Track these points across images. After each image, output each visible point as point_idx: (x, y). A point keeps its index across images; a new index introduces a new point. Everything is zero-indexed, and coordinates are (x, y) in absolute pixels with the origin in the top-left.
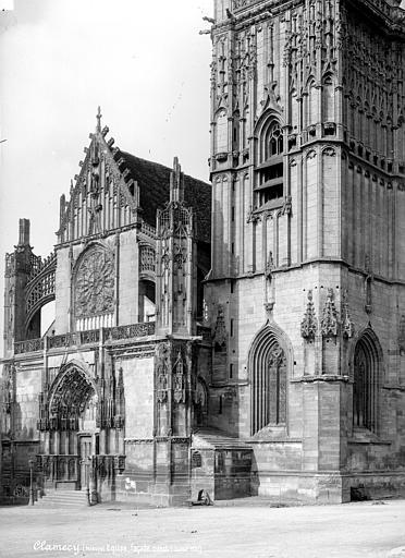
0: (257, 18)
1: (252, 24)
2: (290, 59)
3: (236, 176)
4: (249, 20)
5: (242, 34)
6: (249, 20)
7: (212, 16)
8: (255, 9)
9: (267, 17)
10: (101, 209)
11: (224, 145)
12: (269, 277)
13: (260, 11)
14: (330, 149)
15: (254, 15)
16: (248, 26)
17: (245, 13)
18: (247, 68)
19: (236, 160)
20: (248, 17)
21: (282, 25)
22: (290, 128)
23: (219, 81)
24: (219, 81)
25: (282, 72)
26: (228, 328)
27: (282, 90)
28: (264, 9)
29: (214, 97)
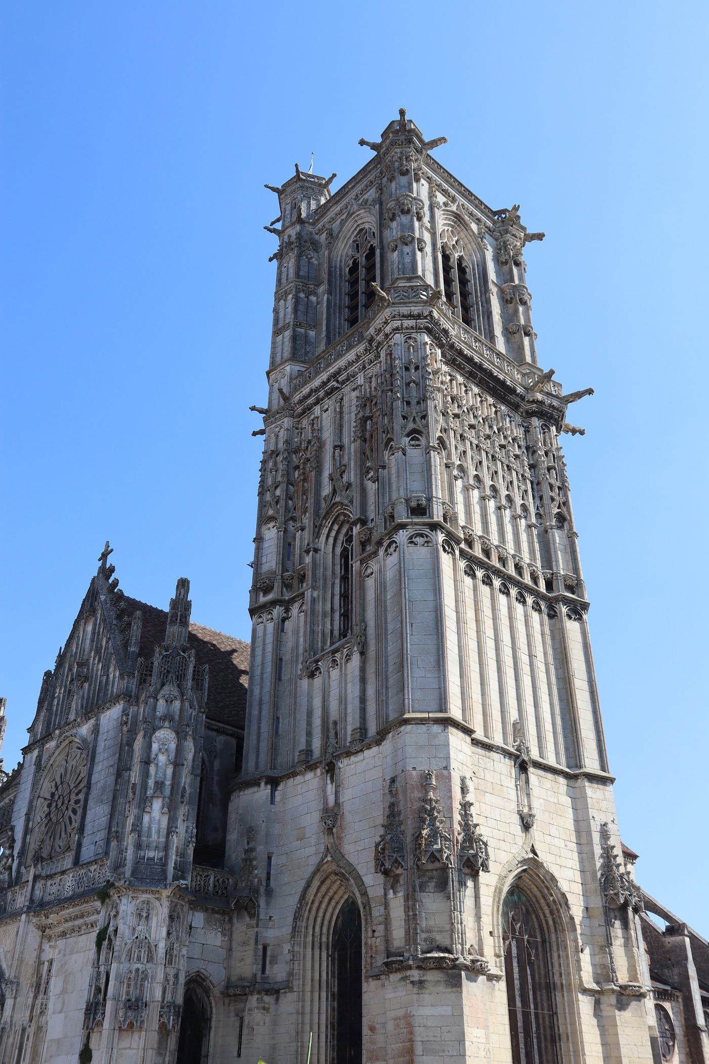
0: (321, 393)
2: (364, 430)
3: (287, 610)
5: (305, 422)
7: (266, 407)
8: (316, 383)
9: (333, 389)
11: (271, 562)
12: (331, 770)
13: (324, 384)
14: (421, 535)
15: (317, 390)
16: (310, 408)
18: (308, 460)
19: (287, 586)
20: (309, 395)
21: (354, 394)
22: (363, 522)
23: (270, 481)
24: (270, 481)
26: (260, 872)
27: (352, 476)
28: (329, 380)
29: (262, 505)
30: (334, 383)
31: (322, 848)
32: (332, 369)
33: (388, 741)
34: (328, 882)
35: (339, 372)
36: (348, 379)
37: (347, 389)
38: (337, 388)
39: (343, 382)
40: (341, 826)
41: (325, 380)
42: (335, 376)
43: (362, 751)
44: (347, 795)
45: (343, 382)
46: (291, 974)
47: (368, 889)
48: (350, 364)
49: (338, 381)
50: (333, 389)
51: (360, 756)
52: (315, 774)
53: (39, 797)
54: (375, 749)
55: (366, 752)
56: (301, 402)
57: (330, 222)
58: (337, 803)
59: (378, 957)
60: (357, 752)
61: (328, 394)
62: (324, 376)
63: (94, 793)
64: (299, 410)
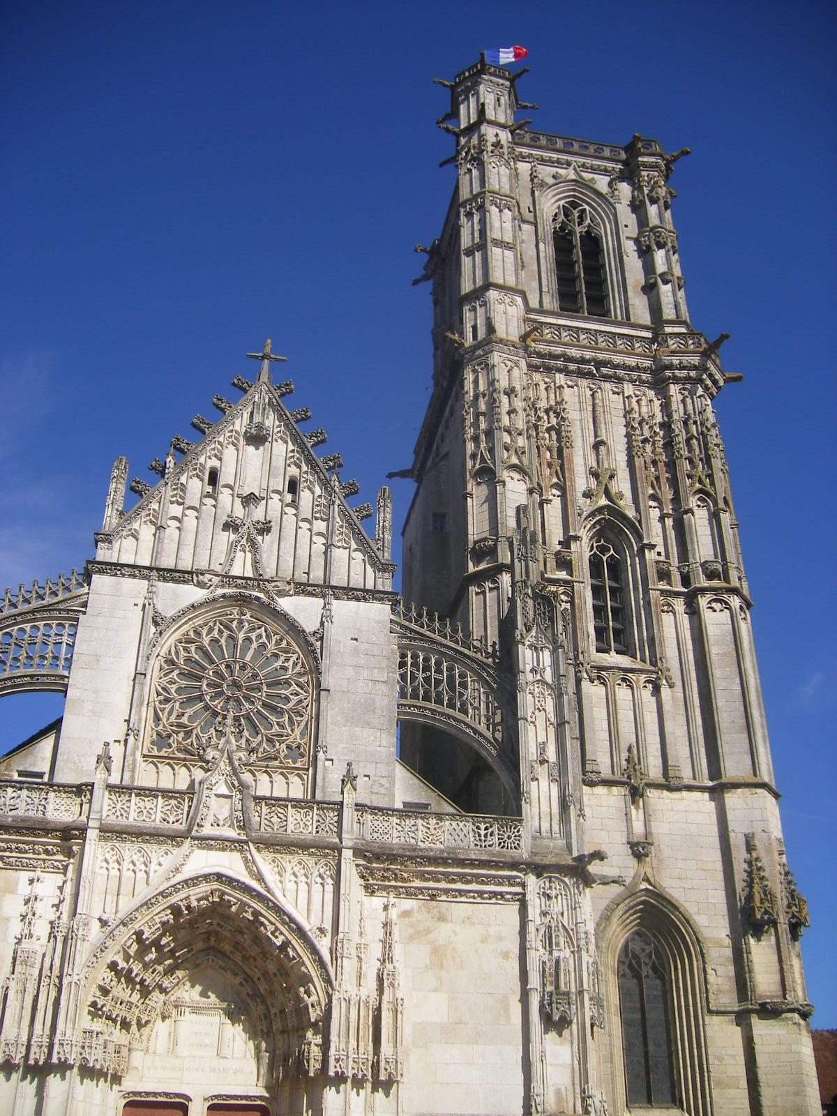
0: (573, 367)
1: (560, 371)
4: (560, 363)
6: (560, 363)
8: (574, 353)
10: (269, 530)
13: (583, 361)
17: (559, 350)
25: (619, 459)
32: (601, 356)
33: (735, 796)
35: (605, 364)
36: (611, 377)
38: (595, 375)
42: (599, 364)
44: (660, 829)
48: (625, 367)
51: (676, 795)
52: (610, 792)
53: (158, 655)
56: (540, 355)
57: (537, 159)
58: (647, 834)
61: (581, 374)
62: (588, 355)
64: (536, 361)
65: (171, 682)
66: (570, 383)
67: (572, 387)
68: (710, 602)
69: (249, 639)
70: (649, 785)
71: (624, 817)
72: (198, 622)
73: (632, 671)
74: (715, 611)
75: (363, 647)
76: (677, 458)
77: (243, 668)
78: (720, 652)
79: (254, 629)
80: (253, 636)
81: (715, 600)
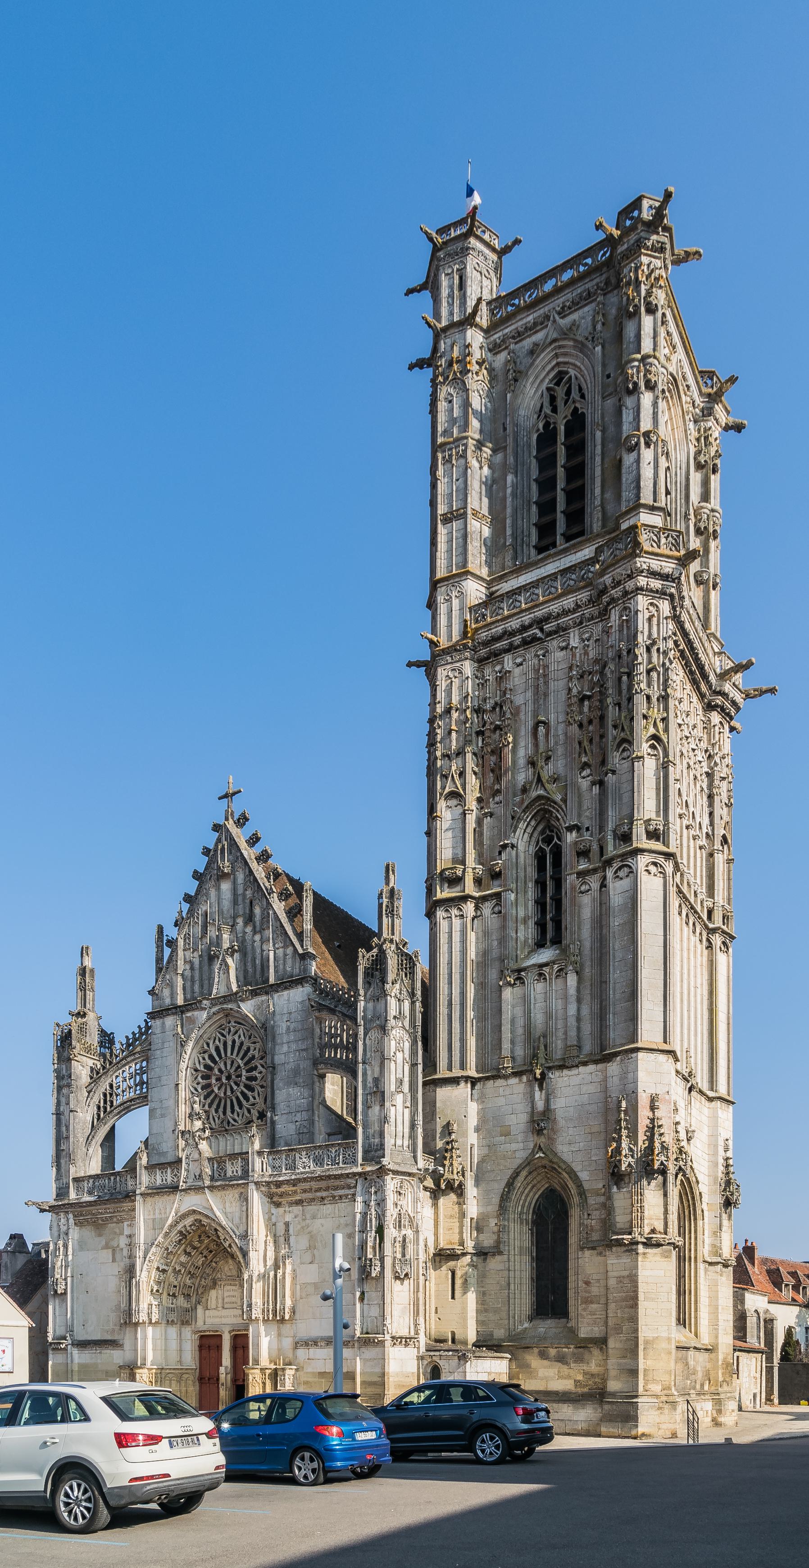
8: (514, 624)
9: (534, 639)
13: (524, 628)
17: (498, 629)
28: (530, 626)
30: (537, 631)
31: (531, 1145)
34: (535, 1173)
37: (554, 644)
38: (540, 639)
39: (549, 634)
40: (552, 1129)
41: (526, 623)
43: (577, 1066)
45: (549, 634)
46: (498, 1242)
47: (584, 1183)
49: (542, 630)
50: (534, 639)
54: (591, 1068)
55: (582, 1069)
59: (593, 1234)
60: (573, 1067)
63: (281, 1075)
65: (198, 1084)
66: (519, 660)
67: (521, 664)
68: (616, 872)
69: (234, 1042)
70: (550, 1068)
71: (529, 1100)
72: (205, 1036)
73: (546, 965)
74: (621, 879)
75: (292, 1026)
76: (637, 693)
77: (232, 1062)
78: (622, 922)
79: (236, 1032)
80: (236, 1037)
81: (620, 868)
